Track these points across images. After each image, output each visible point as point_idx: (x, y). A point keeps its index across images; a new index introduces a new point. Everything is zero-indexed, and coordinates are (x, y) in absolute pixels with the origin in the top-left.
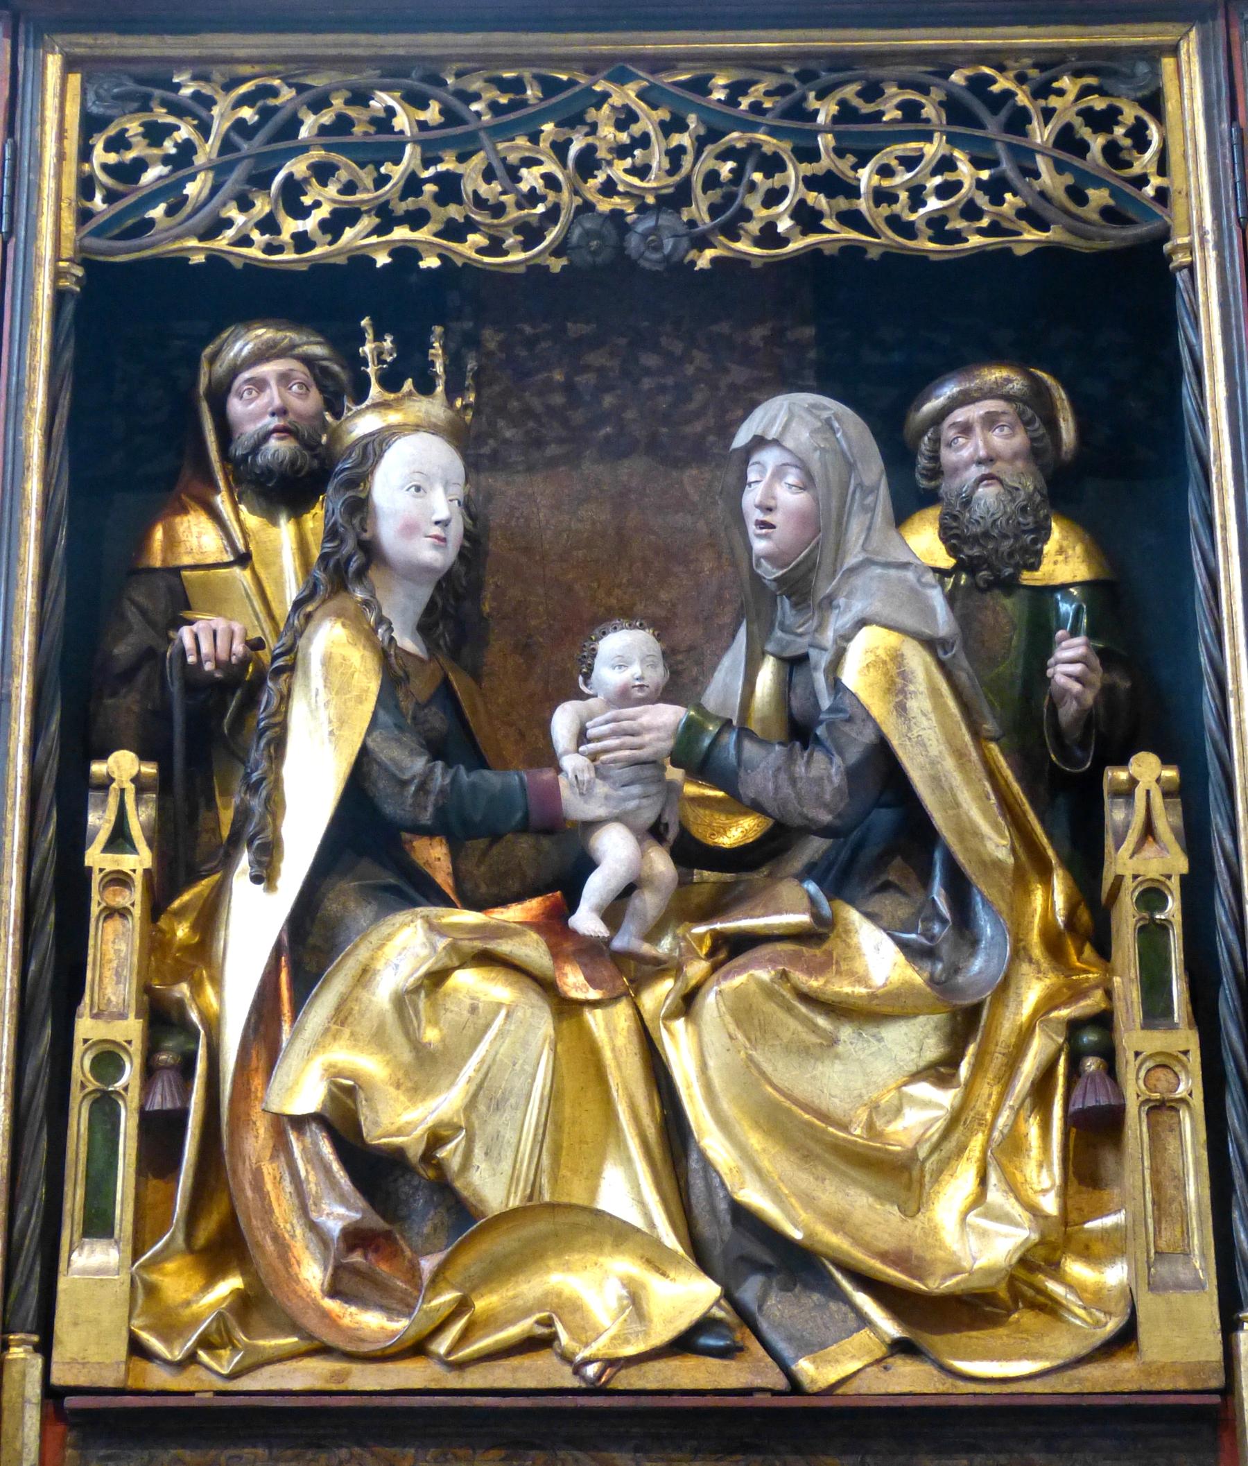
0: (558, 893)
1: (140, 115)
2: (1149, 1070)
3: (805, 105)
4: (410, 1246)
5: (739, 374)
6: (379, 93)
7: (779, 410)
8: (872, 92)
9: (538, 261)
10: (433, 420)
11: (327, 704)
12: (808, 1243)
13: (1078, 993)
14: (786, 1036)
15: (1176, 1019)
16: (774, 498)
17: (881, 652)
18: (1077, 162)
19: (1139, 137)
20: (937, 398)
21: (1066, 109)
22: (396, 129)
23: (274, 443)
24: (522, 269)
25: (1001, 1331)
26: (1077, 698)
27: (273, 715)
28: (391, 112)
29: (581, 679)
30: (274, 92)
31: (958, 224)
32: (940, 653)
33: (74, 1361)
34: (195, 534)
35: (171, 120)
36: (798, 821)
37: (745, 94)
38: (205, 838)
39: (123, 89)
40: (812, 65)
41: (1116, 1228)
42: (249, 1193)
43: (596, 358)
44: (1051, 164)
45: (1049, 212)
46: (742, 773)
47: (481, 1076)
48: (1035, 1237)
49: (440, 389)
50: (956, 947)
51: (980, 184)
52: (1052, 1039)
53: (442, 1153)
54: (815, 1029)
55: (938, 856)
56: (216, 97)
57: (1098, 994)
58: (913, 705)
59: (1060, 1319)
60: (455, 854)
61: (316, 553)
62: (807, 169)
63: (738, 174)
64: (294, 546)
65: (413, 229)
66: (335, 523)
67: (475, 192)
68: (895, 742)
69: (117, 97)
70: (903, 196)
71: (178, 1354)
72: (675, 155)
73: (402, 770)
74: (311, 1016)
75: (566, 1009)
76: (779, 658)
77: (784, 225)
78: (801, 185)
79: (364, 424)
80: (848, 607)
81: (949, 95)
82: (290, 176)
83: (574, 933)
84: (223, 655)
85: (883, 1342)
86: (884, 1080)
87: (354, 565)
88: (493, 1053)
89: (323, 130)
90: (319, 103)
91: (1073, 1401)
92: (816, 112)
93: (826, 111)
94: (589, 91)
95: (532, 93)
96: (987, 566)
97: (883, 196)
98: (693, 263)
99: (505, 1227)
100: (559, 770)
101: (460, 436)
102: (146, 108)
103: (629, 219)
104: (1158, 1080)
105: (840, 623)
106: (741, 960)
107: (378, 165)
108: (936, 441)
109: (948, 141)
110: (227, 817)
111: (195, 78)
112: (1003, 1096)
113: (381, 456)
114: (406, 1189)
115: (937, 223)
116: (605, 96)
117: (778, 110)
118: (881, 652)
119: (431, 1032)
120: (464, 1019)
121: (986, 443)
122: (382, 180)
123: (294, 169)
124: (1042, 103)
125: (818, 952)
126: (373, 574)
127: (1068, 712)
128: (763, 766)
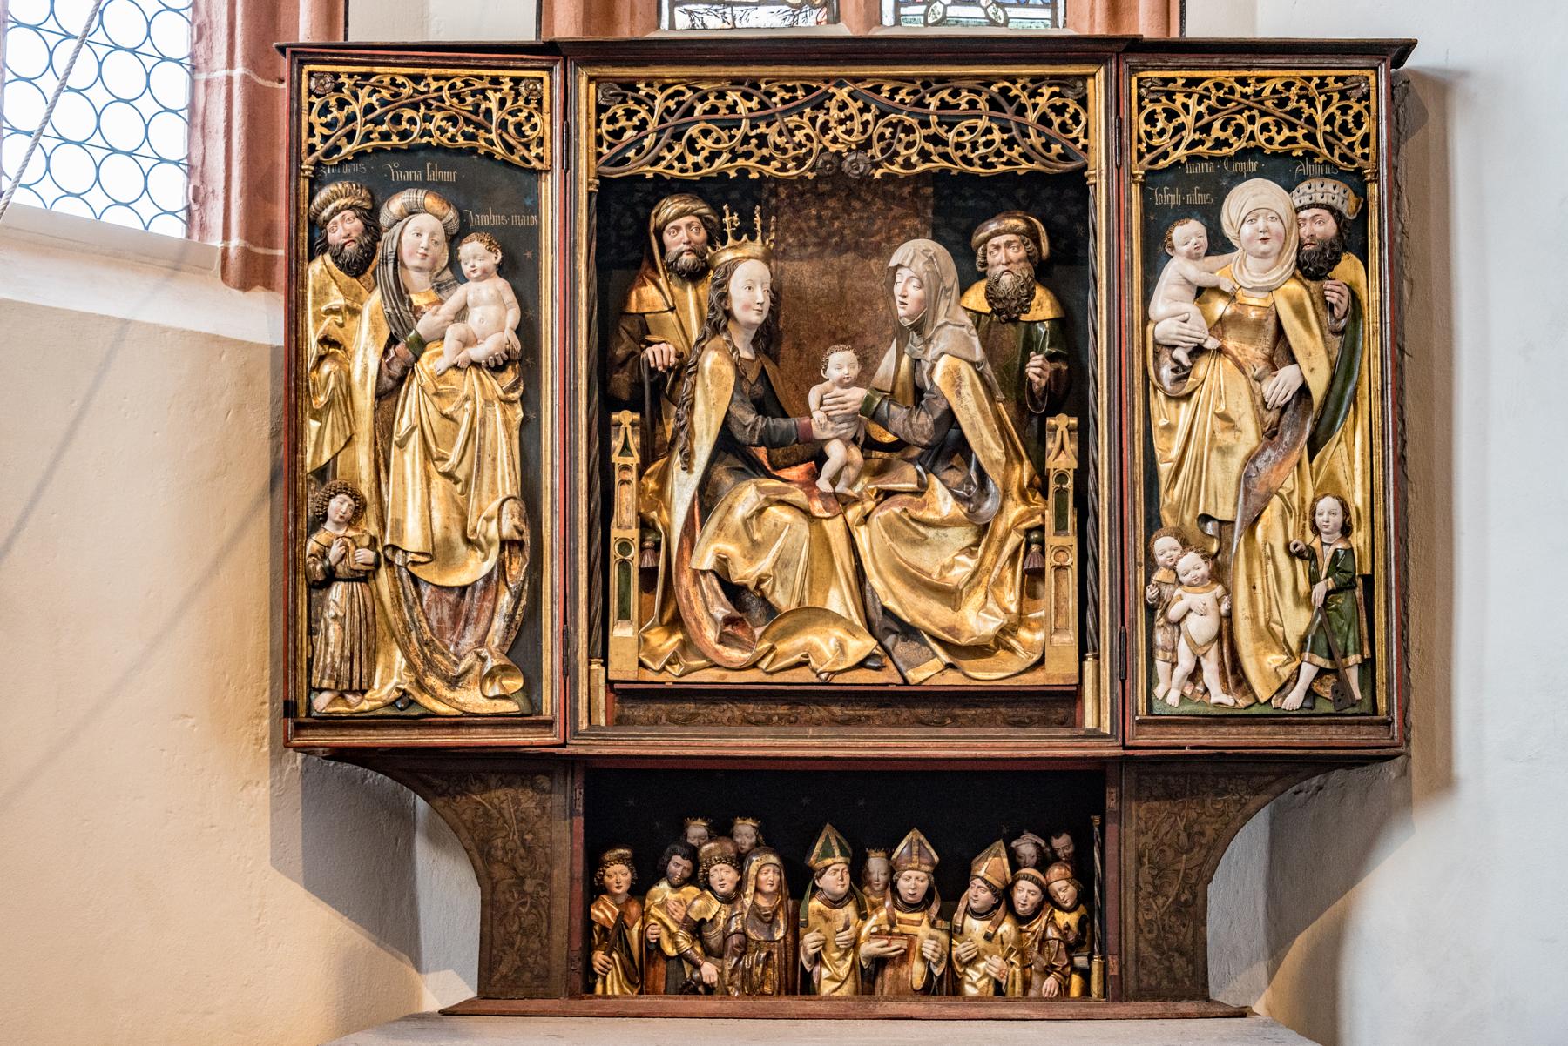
8: (955, 93)
13: (1032, 515)
19: (1076, 118)
28: (735, 102)
30: (682, 93)
31: (994, 160)
35: (636, 107)
51: (1003, 141)
54: (918, 533)
62: (925, 132)
63: (893, 134)
72: (865, 124)
77: (914, 159)
89: (705, 112)
90: (703, 99)
93: (934, 102)
101: (767, 258)
102: (624, 101)
115: (983, 158)
122: (732, 138)
128: (898, 414)
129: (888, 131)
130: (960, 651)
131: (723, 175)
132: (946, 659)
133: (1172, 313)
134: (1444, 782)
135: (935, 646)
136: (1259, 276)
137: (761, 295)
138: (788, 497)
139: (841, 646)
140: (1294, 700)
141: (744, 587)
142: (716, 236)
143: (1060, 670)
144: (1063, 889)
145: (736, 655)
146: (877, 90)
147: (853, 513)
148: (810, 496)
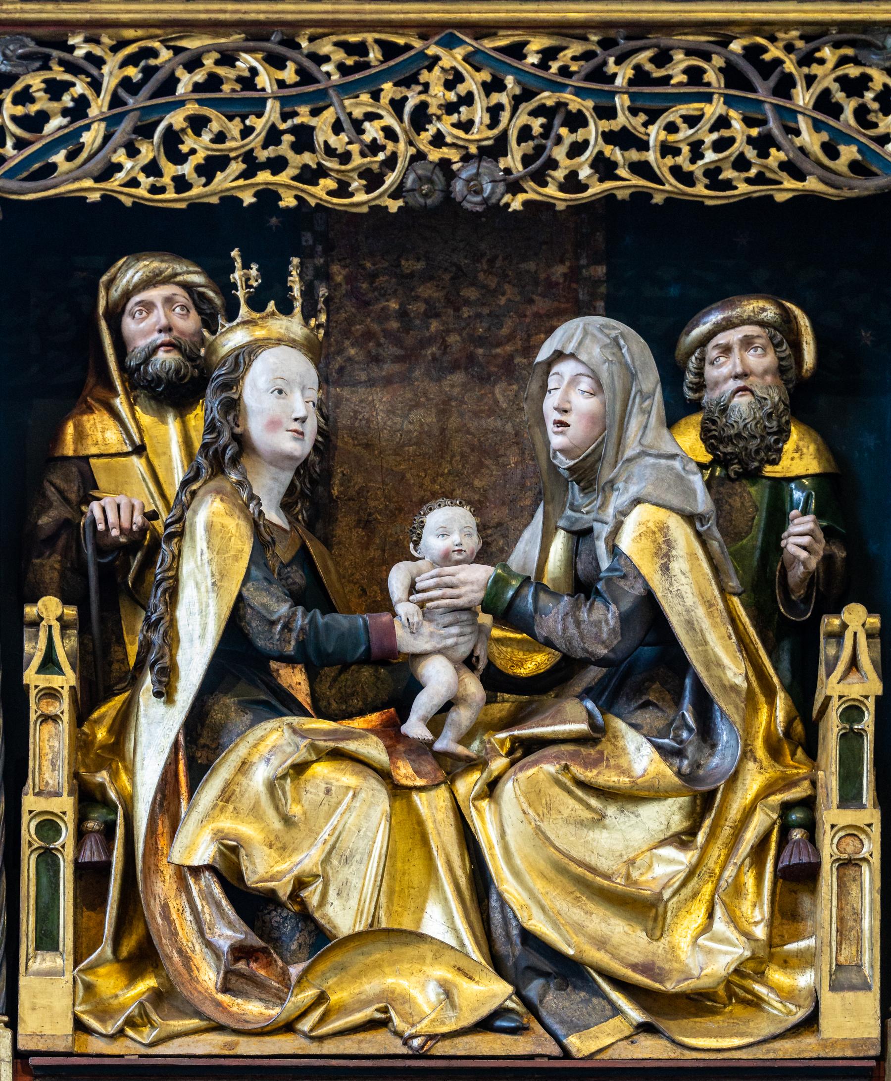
0: (392, 710)
1: (42, 73)
2: (841, 838)
3: (605, 69)
4: (281, 958)
5: (542, 305)
6: (243, 55)
7: (576, 329)
8: (663, 58)
9: (377, 202)
10: (292, 336)
11: (210, 561)
12: (578, 956)
13: (791, 783)
14: (566, 813)
15: (864, 801)
16: (569, 402)
17: (651, 525)
18: (832, 122)
20: (704, 324)
21: (826, 76)
22: (259, 87)
23: (161, 355)
24: (365, 209)
25: (718, 1018)
26: (804, 563)
27: (169, 569)
28: (254, 71)
29: (411, 545)
30: (154, 54)
32: (698, 525)
33: (33, 1035)
34: (99, 429)
35: (68, 77)
36: (580, 654)
37: (555, 59)
38: (116, 666)
39: (27, 49)
40: (612, 33)
41: (808, 948)
42: (160, 921)
43: (427, 291)
44: (810, 122)
45: (805, 165)
46: (537, 618)
47: (334, 838)
48: (748, 954)
49: (298, 310)
50: (699, 749)
51: (750, 140)
52: (768, 815)
53: (304, 894)
54: (588, 807)
55: (688, 682)
56: (106, 57)
57: (806, 784)
58: (676, 566)
59: (761, 1009)
60: (312, 678)
61: (197, 445)
62: (605, 125)
63: (547, 129)
64: (180, 440)
65: (274, 174)
66: (213, 419)
67: (326, 143)
68: (659, 594)
69: (21, 57)
70: (686, 149)
71: (110, 1030)
72: (495, 111)
73: (272, 613)
74: (203, 795)
75: (398, 792)
76: (567, 531)
77: (585, 173)
78: (600, 140)
79: (234, 338)
80: (626, 489)
81: (728, 62)
82: (170, 127)
83: (406, 737)
84: (126, 524)
85: (631, 1024)
86: (638, 841)
87: (229, 453)
88: (342, 823)
90: (193, 64)
91: (768, 1064)
92: (615, 75)
93: (623, 74)
94: (422, 54)
95: (374, 55)
96: (735, 460)
97: (668, 150)
98: (508, 205)
99: (352, 945)
100: (395, 615)
101: (315, 350)
102: (46, 67)
103: (455, 167)
104: (848, 844)
105: (619, 501)
106: (532, 758)
107: (244, 118)
108: (702, 360)
109: (725, 103)
110: (132, 650)
111: (87, 40)
112: (728, 857)
113: (250, 365)
114: (278, 919)
115: (712, 173)
116: (437, 59)
117: (583, 73)
118: (651, 525)
120: (319, 799)
121: (742, 361)
122: (247, 132)
123: (173, 121)
124: (805, 70)
125: (592, 752)
126: (244, 460)
127: (797, 573)
128: (555, 617)
129: (537, 124)
130: (664, 1005)
131: (230, 202)
132: (636, 1015)
135: (617, 997)
137: (300, 404)
138: (351, 746)
139: (448, 994)
141: (270, 898)
145: (254, 1009)
146: (517, 51)
147: (468, 785)
148: (391, 751)
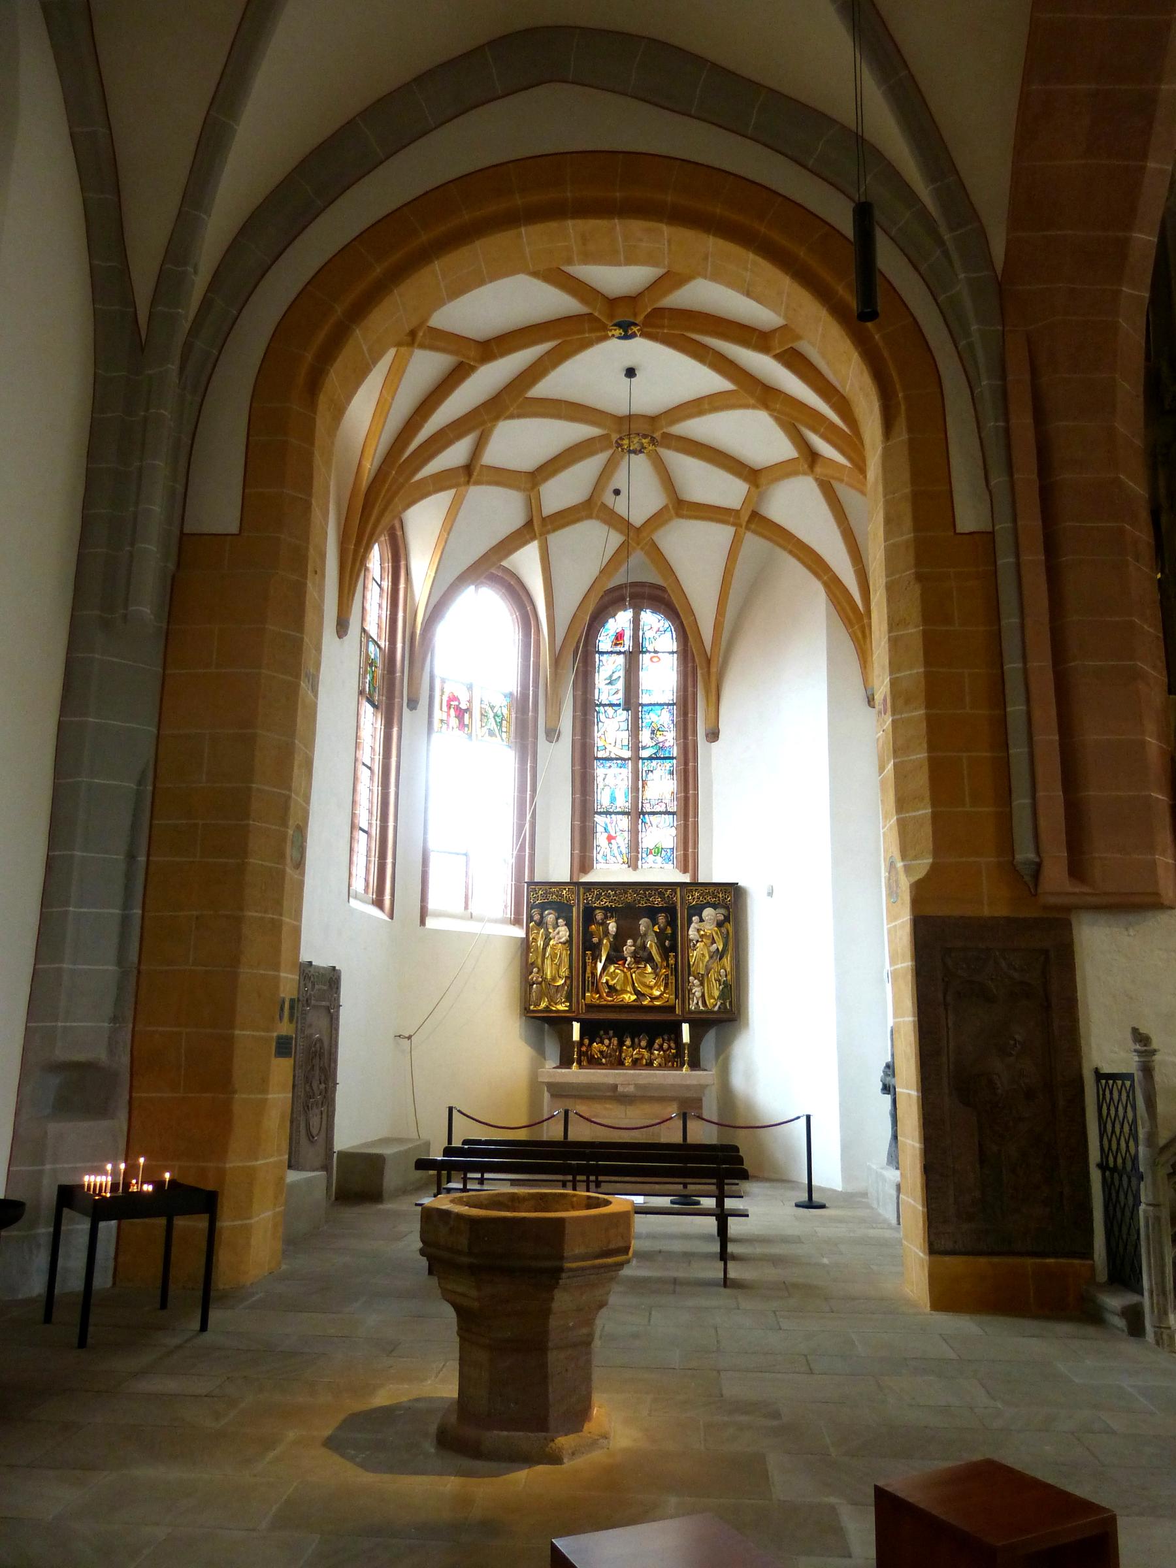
119: (614, 975)
133: (692, 933)
134: (747, 1024)
136: (709, 928)
140: (716, 1008)
142: (606, 917)
143: (671, 1002)
144: (673, 1045)
